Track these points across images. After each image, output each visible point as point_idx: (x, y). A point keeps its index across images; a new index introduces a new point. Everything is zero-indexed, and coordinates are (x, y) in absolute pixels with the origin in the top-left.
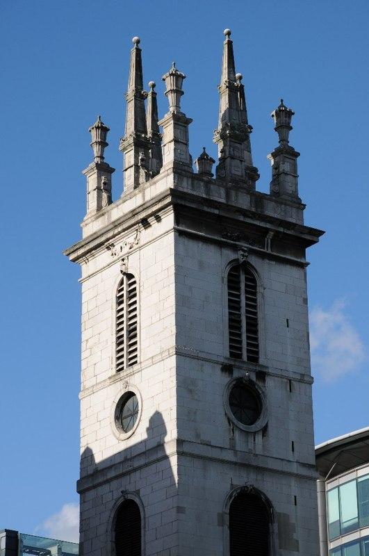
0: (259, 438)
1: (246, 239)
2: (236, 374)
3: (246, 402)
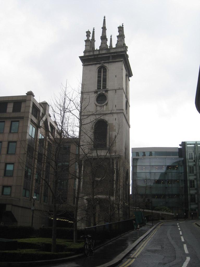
0: (105, 107)
1: (104, 60)
2: (99, 93)
3: (101, 98)
